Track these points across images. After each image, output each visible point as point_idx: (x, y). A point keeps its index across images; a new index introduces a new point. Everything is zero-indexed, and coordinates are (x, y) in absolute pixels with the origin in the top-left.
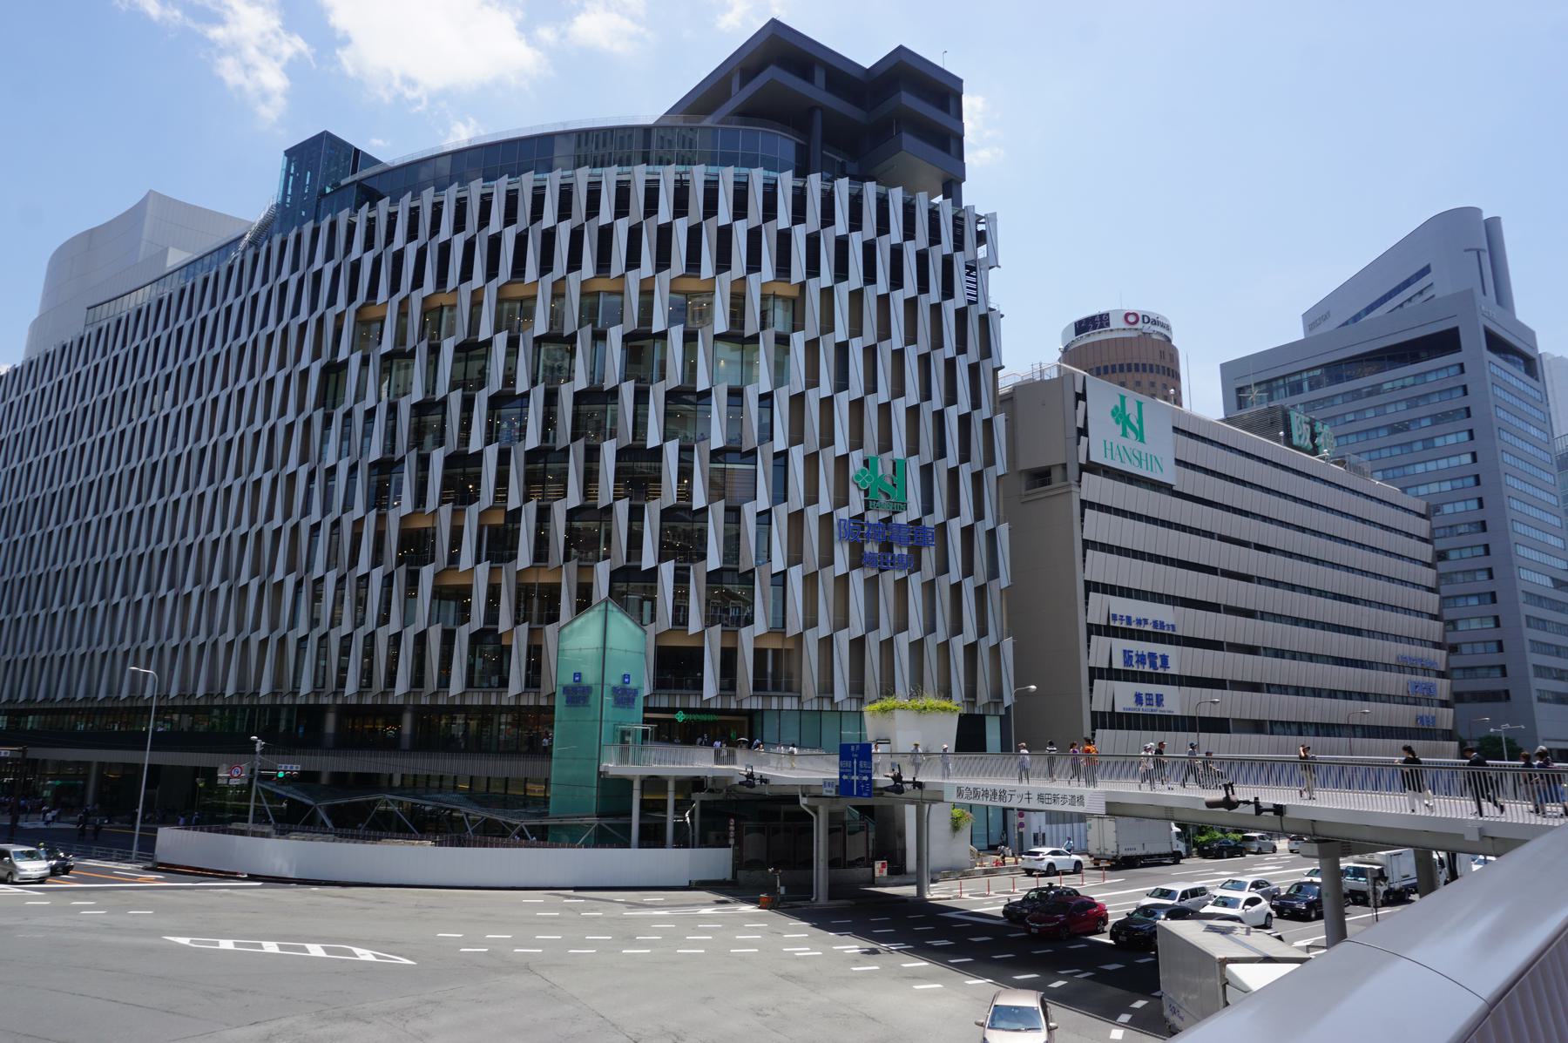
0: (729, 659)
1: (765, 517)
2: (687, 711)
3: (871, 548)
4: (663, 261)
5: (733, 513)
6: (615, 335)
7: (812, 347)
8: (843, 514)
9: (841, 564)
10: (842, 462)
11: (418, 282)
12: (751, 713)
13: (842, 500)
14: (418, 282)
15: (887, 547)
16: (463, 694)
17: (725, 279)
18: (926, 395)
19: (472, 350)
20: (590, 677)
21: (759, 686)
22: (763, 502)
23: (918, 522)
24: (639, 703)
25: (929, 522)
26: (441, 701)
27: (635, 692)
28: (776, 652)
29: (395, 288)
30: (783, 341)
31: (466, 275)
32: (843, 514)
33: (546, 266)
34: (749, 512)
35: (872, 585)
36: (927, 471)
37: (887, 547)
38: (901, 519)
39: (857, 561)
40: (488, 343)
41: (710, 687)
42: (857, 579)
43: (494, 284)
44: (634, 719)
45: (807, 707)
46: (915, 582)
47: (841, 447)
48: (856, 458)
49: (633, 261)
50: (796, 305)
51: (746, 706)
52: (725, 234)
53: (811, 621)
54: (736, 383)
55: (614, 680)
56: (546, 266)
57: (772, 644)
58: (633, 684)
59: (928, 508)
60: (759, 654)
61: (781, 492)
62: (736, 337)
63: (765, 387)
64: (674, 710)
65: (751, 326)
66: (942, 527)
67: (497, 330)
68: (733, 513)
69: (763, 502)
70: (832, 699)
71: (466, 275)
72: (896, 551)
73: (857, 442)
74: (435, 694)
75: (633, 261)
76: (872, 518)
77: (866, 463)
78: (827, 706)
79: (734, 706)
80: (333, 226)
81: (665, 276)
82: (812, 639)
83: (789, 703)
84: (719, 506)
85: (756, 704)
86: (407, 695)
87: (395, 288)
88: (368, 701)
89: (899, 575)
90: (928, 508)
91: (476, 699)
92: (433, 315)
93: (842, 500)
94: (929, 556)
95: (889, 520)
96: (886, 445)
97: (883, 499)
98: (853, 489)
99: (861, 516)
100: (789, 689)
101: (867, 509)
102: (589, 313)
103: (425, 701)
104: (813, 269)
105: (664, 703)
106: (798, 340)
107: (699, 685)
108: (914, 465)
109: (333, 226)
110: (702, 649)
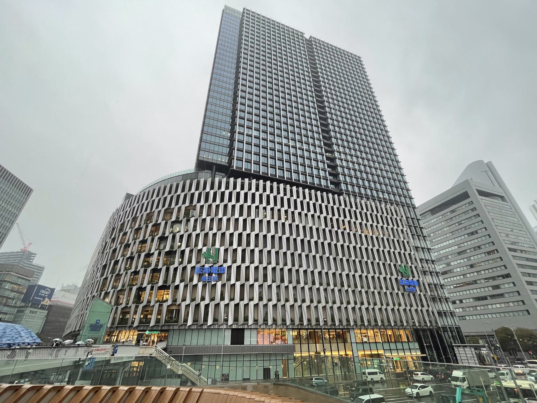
0: (160, 312)
1: (176, 269)
2: (149, 331)
8: (198, 266)
9: (195, 281)
10: (200, 250)
13: (198, 262)
15: (210, 274)
23: (222, 266)
25: (225, 266)
32: (198, 266)
34: (172, 268)
35: (204, 286)
37: (210, 274)
38: (217, 265)
42: (200, 285)
45: (181, 328)
46: (219, 284)
47: (200, 246)
48: (205, 249)
51: (163, 328)
53: (184, 300)
57: (174, 308)
59: (225, 261)
60: (169, 311)
64: (146, 331)
66: (230, 267)
68: (168, 269)
72: (214, 275)
76: (207, 266)
78: (187, 328)
82: (183, 305)
85: (165, 328)
89: (213, 283)
90: (225, 261)
94: (225, 276)
95: (213, 266)
96: (214, 244)
99: (203, 266)
106: (192, 220)
108: (222, 249)
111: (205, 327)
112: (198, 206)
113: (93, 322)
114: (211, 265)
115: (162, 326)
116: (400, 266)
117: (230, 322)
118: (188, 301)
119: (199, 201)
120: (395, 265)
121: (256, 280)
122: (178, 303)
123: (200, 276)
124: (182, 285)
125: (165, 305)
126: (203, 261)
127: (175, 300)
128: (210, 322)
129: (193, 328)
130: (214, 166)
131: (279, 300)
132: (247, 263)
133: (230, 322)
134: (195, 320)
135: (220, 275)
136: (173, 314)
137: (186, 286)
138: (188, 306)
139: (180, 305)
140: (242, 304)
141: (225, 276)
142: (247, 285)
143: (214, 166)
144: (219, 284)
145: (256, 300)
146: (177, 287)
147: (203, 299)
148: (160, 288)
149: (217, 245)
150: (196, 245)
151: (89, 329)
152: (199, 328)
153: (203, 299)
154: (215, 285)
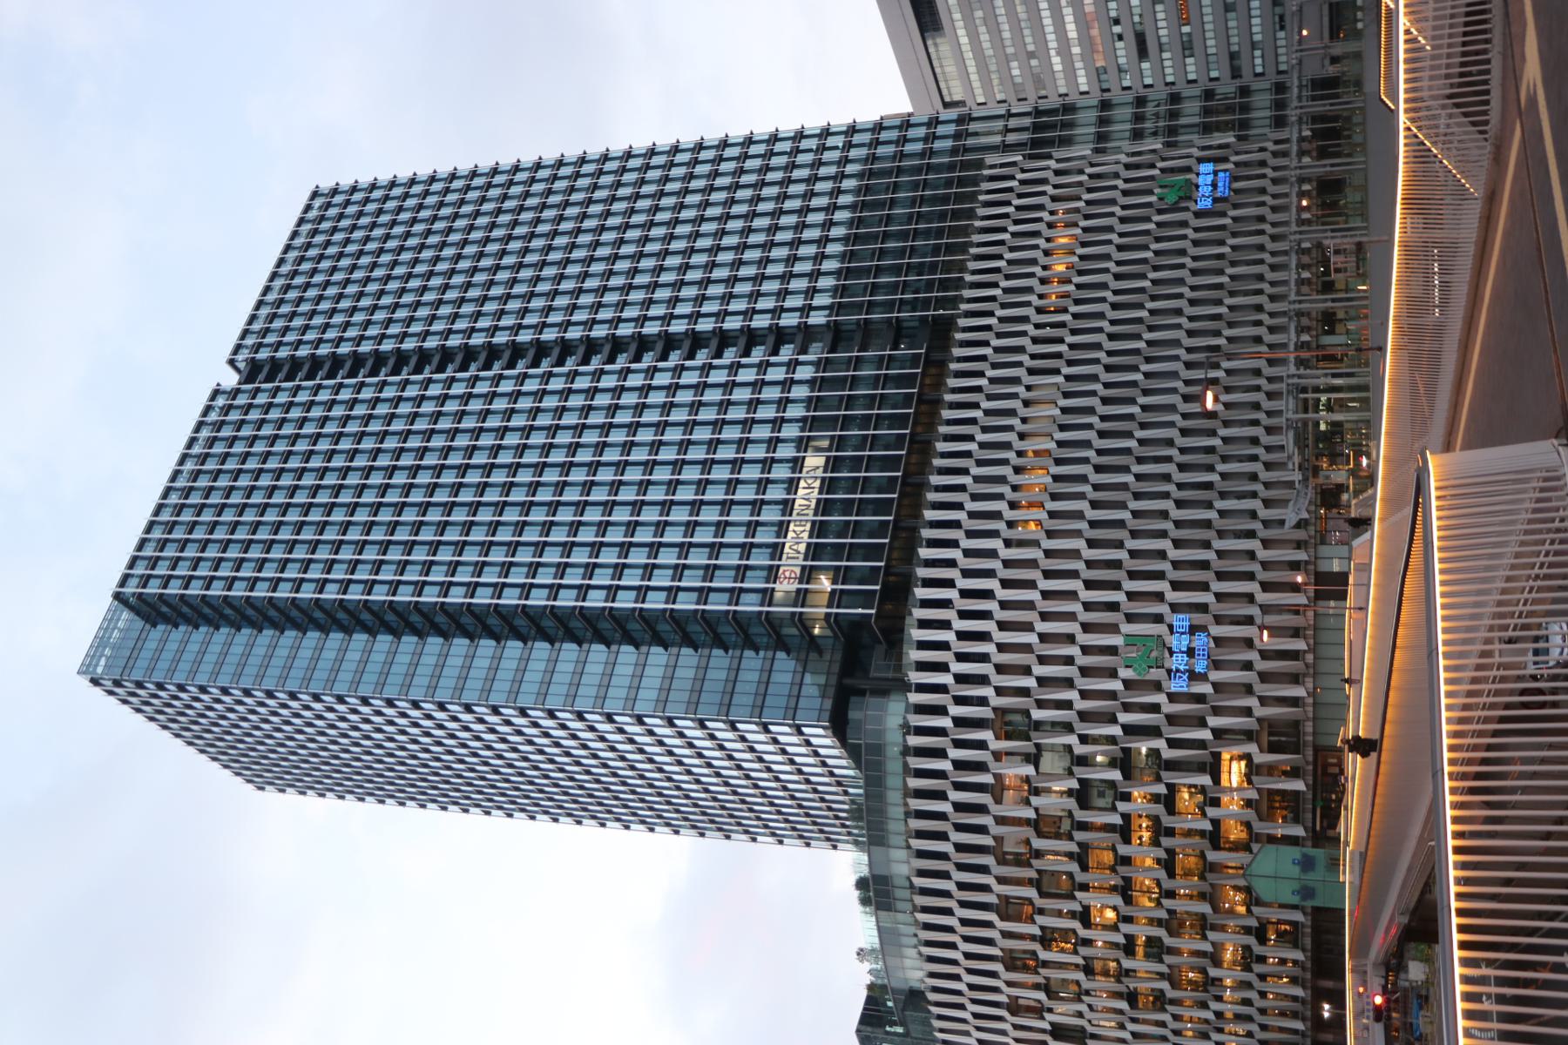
1: (1172, 743)
4: (981, 809)
6: (1038, 843)
10: (1128, 684)
11: (993, 974)
12: (1317, 750)
14: (993, 974)
16: (1304, 950)
17: (992, 764)
18: (1071, 616)
19: (1046, 938)
20: (1296, 886)
24: (1311, 851)
26: (1309, 965)
27: (1305, 856)
28: (1270, 734)
29: (996, 990)
30: (1038, 725)
31: (989, 942)
34: (1168, 754)
36: (1130, 618)
40: (1042, 928)
41: (1299, 785)
44: (1319, 854)
45: (1311, 715)
47: (1117, 685)
48: (1124, 673)
49: (982, 830)
51: (1310, 759)
52: (959, 765)
53: (1248, 712)
55: (1295, 871)
56: (985, 888)
57: (1265, 739)
60: (1273, 748)
62: (1034, 759)
67: (1034, 922)
69: (1160, 744)
71: (989, 942)
74: (1304, 969)
78: (1310, 700)
80: (942, 1031)
81: (993, 808)
82: (1259, 711)
83: (1309, 727)
85: (1310, 752)
86: (1304, 988)
87: (996, 990)
88: (1309, 1013)
91: (1308, 942)
92: (1012, 962)
96: (1112, 650)
97: (1154, 654)
102: (1019, 861)
103: (1308, 976)
105: (1309, 816)
106: (1037, 714)
107: (1297, 793)
108: (1126, 628)
109: (942, 1031)
110: (1269, 790)
111: (1310, 658)
112: (996, 701)
114: (1167, 654)
116: (1161, 199)
117: (1300, 599)
118: (1252, 702)
120: (1160, 212)
121: (1206, 545)
122: (1256, 727)
124: (1213, 721)
125: (1260, 758)
127: (1249, 736)
128: (1300, 645)
129: (1310, 686)
130: (847, 681)
131: (1254, 495)
132: (1165, 566)
133: (1300, 599)
134: (1295, 679)
136: (1280, 737)
137: (1217, 711)
138: (1264, 701)
139: (1259, 720)
140: (1262, 575)
142: (1218, 564)
143: (847, 681)
145: (1254, 545)
147: (1248, 666)
153: (1248, 666)
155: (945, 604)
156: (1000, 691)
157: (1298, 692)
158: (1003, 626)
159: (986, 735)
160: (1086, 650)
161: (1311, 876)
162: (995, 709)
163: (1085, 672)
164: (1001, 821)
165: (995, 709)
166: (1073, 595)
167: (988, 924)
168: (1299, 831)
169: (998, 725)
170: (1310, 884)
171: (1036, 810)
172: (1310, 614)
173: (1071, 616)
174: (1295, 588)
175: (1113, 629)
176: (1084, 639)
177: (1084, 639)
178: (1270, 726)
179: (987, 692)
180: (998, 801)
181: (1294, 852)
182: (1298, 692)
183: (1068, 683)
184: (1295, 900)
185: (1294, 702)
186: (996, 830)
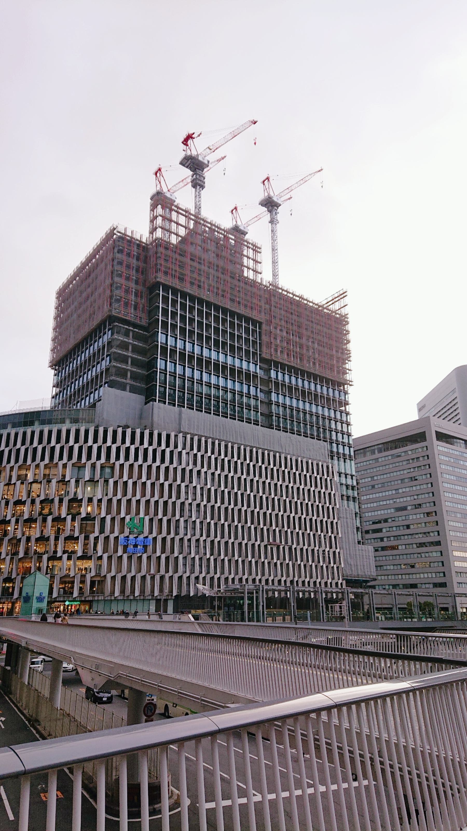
1: (96, 539)
2: (69, 601)
3: (131, 547)
5: (87, 538)
7: (116, 483)
9: (120, 553)
10: (123, 519)
13: (122, 531)
15: (136, 546)
20: (30, 594)
21: (92, 592)
22: (97, 533)
24: (46, 601)
27: (44, 598)
28: (99, 581)
30: (106, 481)
33: (34, 459)
34: (92, 537)
35: (130, 558)
38: (141, 537)
39: (125, 551)
42: (125, 556)
43: (17, 465)
45: (106, 599)
46: (145, 556)
48: (128, 518)
49: (61, 458)
50: (112, 468)
51: (87, 599)
53: (109, 570)
54: (91, 496)
55: (37, 594)
58: (44, 595)
60: (93, 583)
61: (102, 531)
63: (100, 497)
64: (65, 601)
65: (97, 477)
68: (87, 538)
69: (97, 533)
70: (134, 595)
72: (139, 547)
73: (128, 512)
75: (61, 458)
77: (131, 519)
78: (113, 598)
79: (83, 599)
84: (83, 535)
85: (90, 598)
89: (139, 555)
93: (122, 531)
95: (137, 537)
96: (138, 513)
97: (135, 530)
98: (126, 528)
99: (128, 537)
100: (102, 593)
101: (130, 534)
104: (118, 458)
106: (111, 482)
108: (147, 518)
111: (132, 597)
113: (38, 595)
114: (135, 536)
115: (85, 598)
117: (156, 593)
119: (118, 458)
122: (102, 575)
123: (125, 548)
124: (105, 556)
126: (127, 531)
128: (137, 593)
129: (119, 598)
134: (123, 591)
135: (145, 547)
139: (105, 576)
141: (150, 548)
144: (145, 556)
146: (100, 558)
148: (79, 558)
149: (142, 515)
150: (119, 512)
151: (36, 601)
152: (125, 598)
154: (141, 556)
155: (159, 444)
156: (122, 466)
157: (117, 593)
158: (150, 467)
159: (103, 460)
160: (138, 502)
161: (35, 600)
162: (114, 463)
163: (129, 501)
164: (65, 466)
165: (114, 463)
166: (162, 496)
167: (17, 461)
168: (55, 595)
169: (108, 465)
170: (31, 601)
171: (69, 481)
172: (150, 597)
173: (153, 495)
174: (161, 590)
175: (147, 513)
176: (143, 501)
177: (143, 501)
178: (102, 581)
179: (122, 461)
180: (73, 465)
181: (46, 594)
182: (117, 593)
183: (125, 494)
184: (24, 594)
185: (113, 592)
186: (61, 464)
